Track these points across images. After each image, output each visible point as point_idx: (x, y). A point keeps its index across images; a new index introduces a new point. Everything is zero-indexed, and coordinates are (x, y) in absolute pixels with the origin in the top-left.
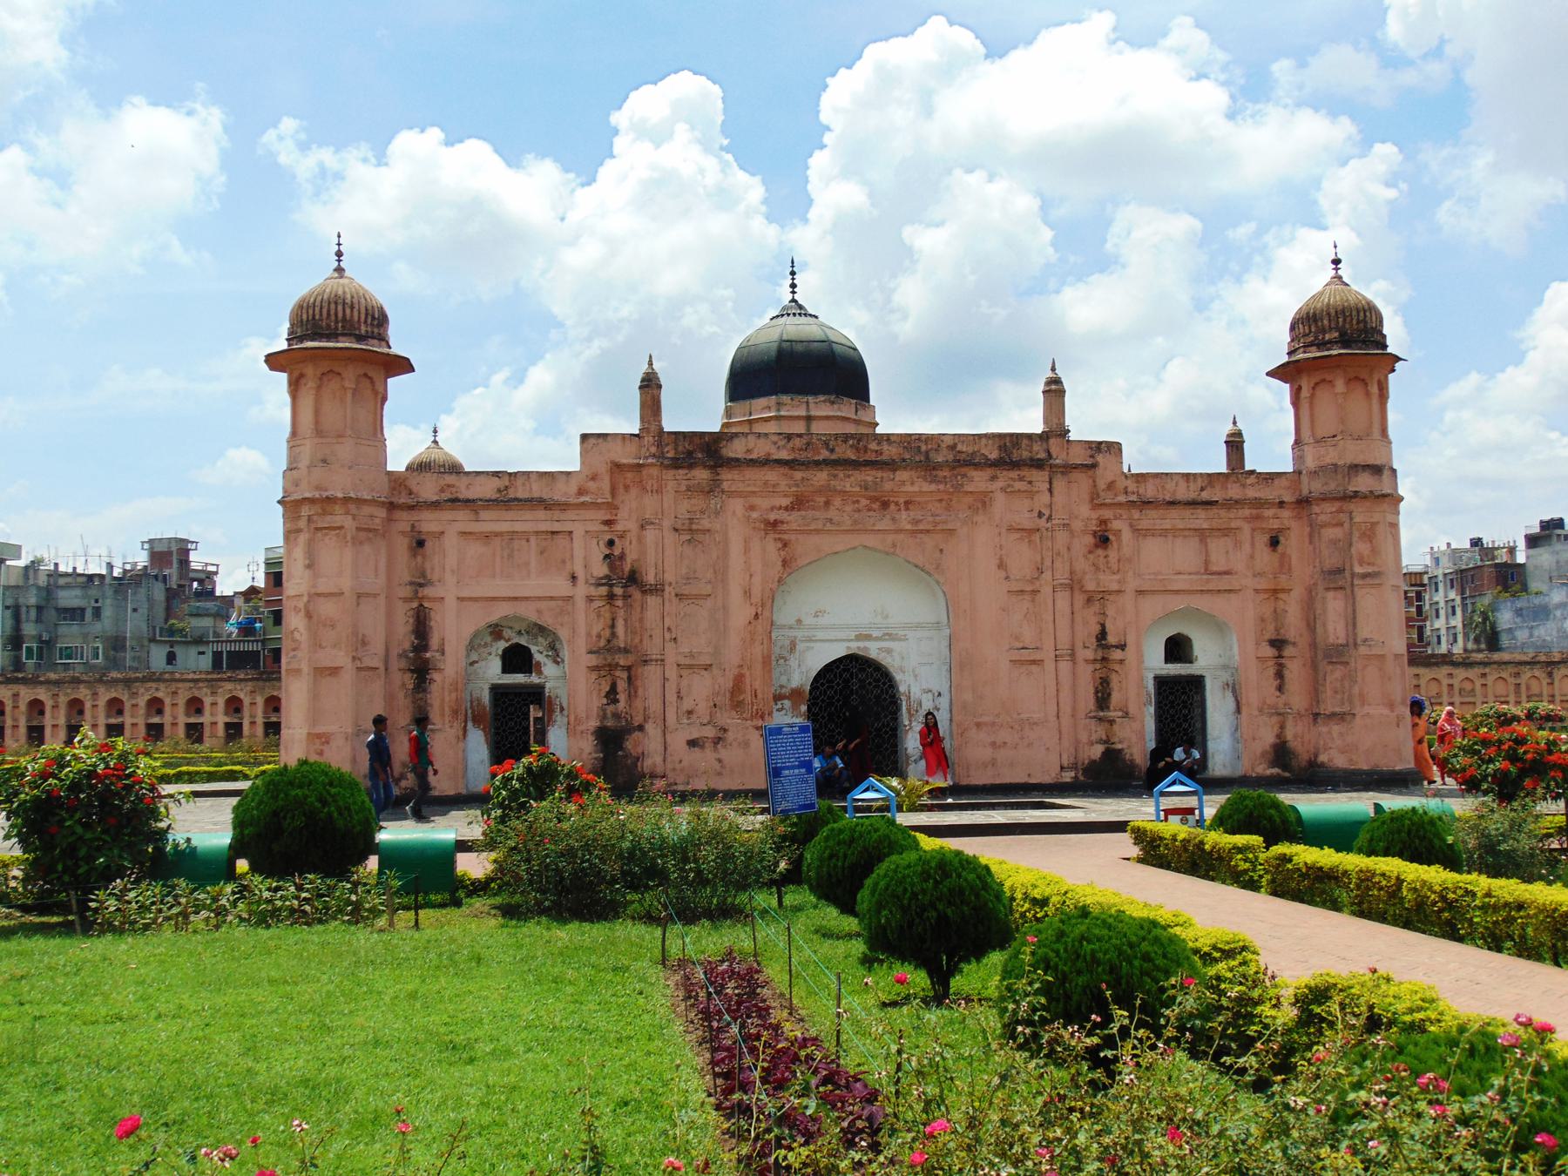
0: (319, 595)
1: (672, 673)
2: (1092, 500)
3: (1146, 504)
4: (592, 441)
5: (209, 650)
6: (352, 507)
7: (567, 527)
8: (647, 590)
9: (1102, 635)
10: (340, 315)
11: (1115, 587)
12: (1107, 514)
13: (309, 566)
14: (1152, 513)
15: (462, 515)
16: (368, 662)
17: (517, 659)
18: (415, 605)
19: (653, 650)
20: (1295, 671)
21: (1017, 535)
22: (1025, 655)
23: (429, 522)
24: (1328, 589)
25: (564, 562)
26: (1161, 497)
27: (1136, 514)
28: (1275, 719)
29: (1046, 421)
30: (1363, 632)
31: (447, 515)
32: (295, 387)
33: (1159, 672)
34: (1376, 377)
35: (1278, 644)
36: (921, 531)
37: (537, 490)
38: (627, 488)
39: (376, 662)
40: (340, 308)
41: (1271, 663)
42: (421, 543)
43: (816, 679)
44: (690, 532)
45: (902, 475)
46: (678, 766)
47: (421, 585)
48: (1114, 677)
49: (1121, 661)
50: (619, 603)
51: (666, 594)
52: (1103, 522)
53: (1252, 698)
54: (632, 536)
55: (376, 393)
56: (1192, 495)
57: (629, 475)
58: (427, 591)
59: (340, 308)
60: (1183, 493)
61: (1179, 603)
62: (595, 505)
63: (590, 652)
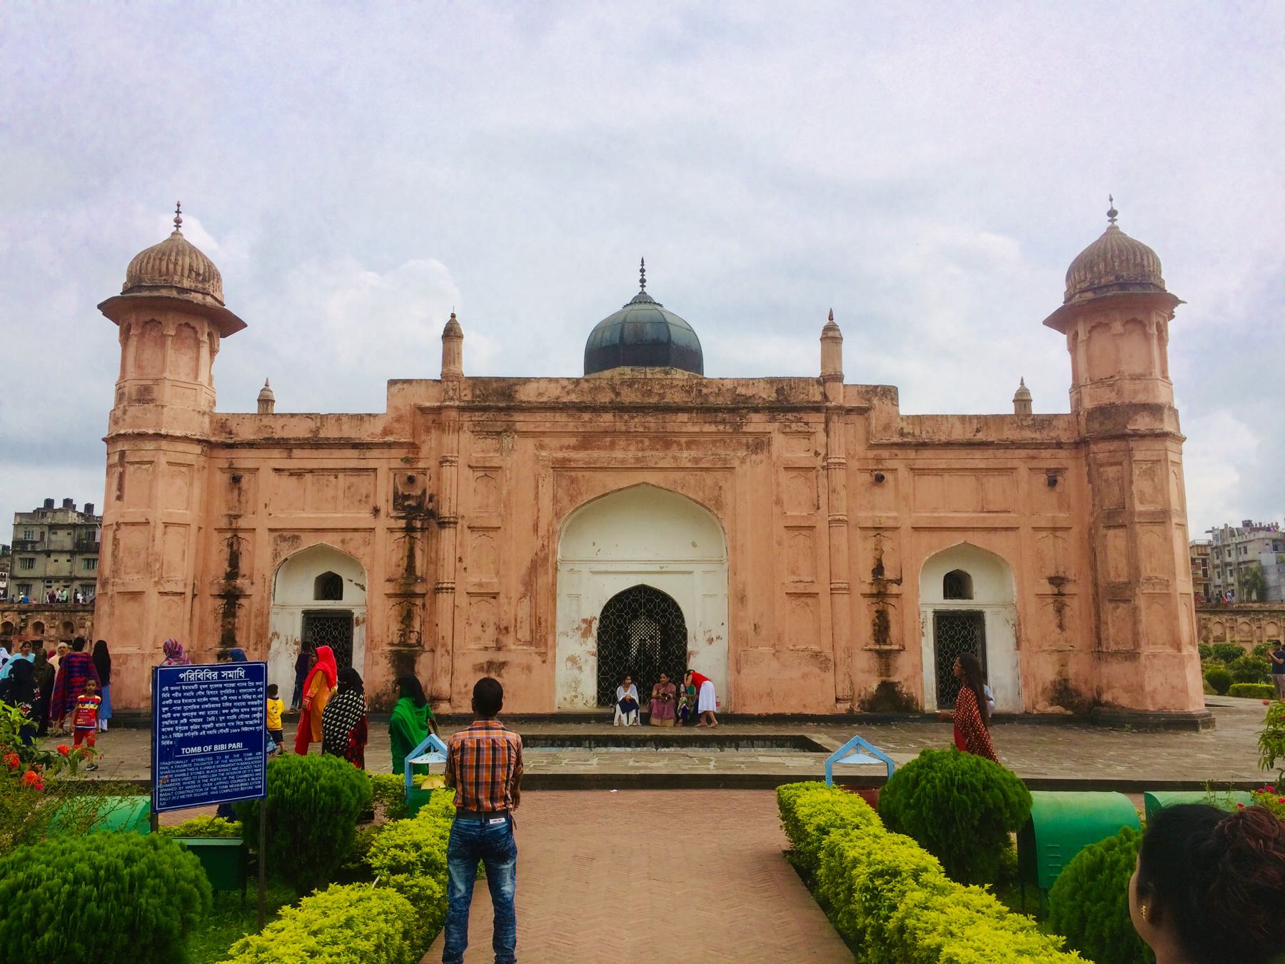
0: (126, 524)
1: (462, 600)
2: (867, 439)
3: (921, 446)
4: (399, 386)
6: (164, 444)
7: (372, 464)
8: (443, 524)
9: (878, 570)
10: (164, 269)
11: (891, 524)
12: (885, 453)
13: (119, 498)
14: (927, 453)
15: (276, 453)
16: (169, 587)
17: (330, 586)
18: (229, 535)
19: (446, 576)
20: (1076, 607)
21: (795, 473)
22: (800, 588)
23: (246, 459)
24: (1108, 527)
25: (367, 496)
26: (936, 438)
27: (912, 454)
28: (1055, 657)
29: (823, 366)
30: (1147, 570)
32: (125, 337)
33: (938, 608)
34: (1155, 319)
36: (702, 469)
37: (349, 432)
38: (428, 430)
40: (164, 263)
41: (1051, 600)
42: (236, 480)
43: (606, 609)
44: (487, 471)
45: (683, 417)
46: (463, 690)
47: (237, 517)
48: (891, 610)
49: (898, 596)
50: (418, 535)
51: (459, 526)
52: (879, 460)
53: (1031, 632)
54: (432, 472)
55: (198, 343)
56: (969, 436)
57: (431, 417)
58: (242, 523)
59: (164, 263)
60: (959, 434)
61: (958, 539)
63: (389, 580)
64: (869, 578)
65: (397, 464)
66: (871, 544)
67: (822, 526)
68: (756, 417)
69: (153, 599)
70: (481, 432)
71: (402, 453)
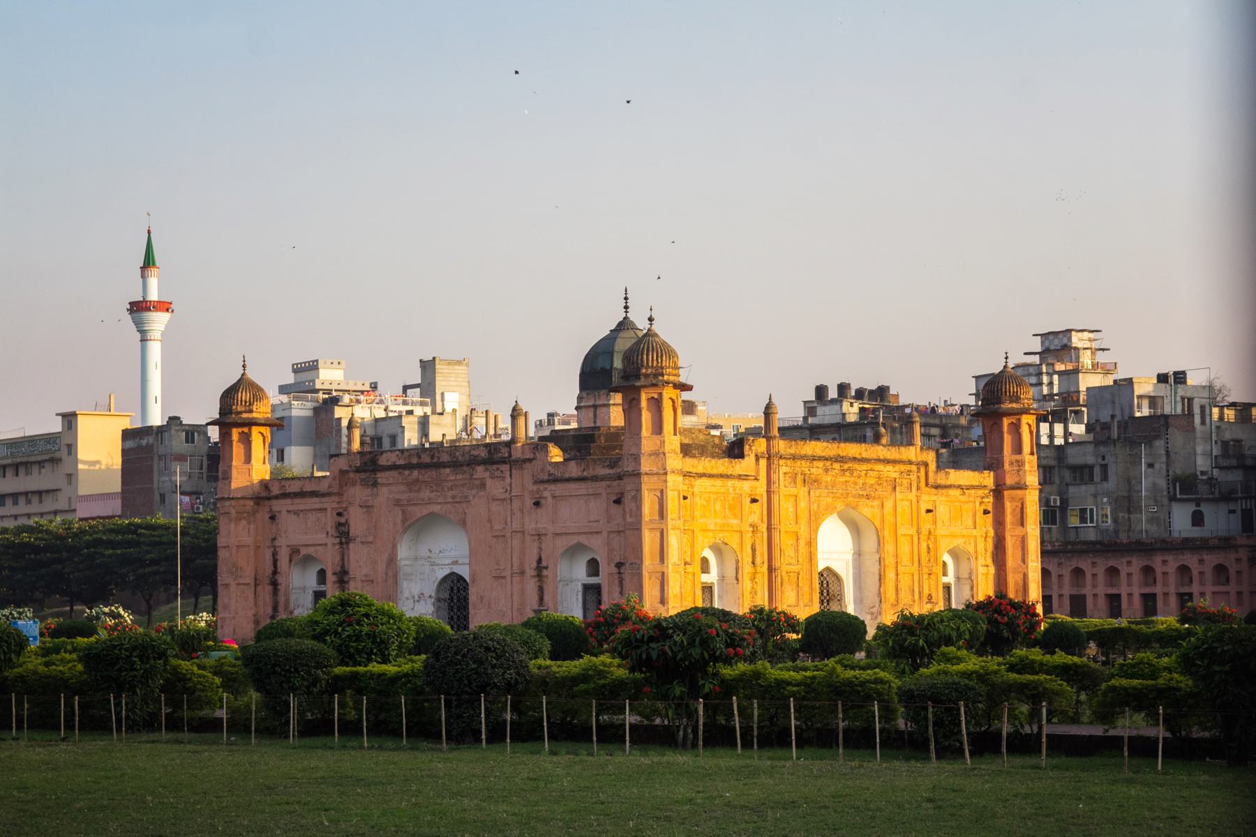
5: (1238, 506)
7: (325, 506)
9: (539, 561)
12: (542, 487)
14: (559, 485)
15: (288, 501)
23: (277, 505)
31: (282, 501)
35: (619, 565)
39: (247, 581)
42: (273, 518)
44: (367, 507)
45: (448, 470)
47: (274, 539)
58: (277, 543)
62: (335, 494)
64: (535, 564)
65: (336, 505)
66: (536, 544)
67: (508, 535)
68: (480, 469)
69: (233, 588)
70: (365, 483)
71: (336, 498)
